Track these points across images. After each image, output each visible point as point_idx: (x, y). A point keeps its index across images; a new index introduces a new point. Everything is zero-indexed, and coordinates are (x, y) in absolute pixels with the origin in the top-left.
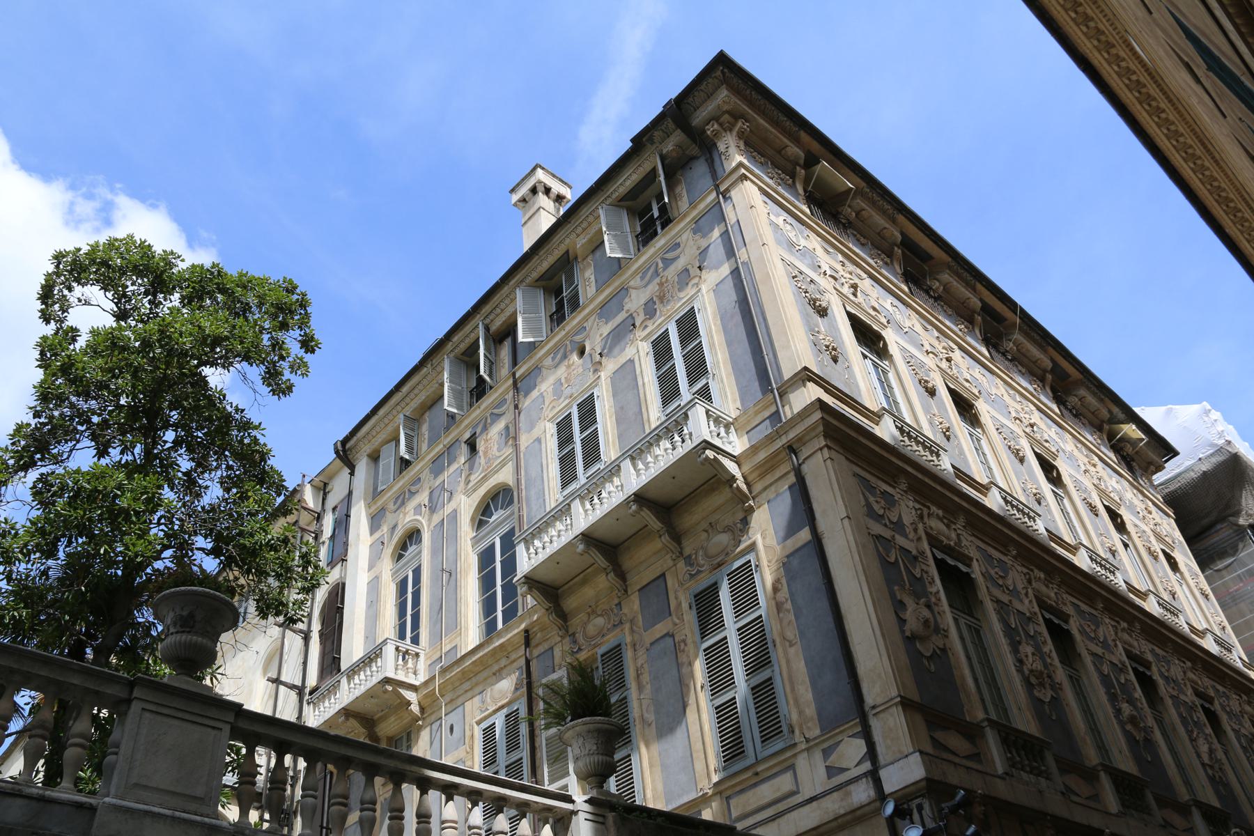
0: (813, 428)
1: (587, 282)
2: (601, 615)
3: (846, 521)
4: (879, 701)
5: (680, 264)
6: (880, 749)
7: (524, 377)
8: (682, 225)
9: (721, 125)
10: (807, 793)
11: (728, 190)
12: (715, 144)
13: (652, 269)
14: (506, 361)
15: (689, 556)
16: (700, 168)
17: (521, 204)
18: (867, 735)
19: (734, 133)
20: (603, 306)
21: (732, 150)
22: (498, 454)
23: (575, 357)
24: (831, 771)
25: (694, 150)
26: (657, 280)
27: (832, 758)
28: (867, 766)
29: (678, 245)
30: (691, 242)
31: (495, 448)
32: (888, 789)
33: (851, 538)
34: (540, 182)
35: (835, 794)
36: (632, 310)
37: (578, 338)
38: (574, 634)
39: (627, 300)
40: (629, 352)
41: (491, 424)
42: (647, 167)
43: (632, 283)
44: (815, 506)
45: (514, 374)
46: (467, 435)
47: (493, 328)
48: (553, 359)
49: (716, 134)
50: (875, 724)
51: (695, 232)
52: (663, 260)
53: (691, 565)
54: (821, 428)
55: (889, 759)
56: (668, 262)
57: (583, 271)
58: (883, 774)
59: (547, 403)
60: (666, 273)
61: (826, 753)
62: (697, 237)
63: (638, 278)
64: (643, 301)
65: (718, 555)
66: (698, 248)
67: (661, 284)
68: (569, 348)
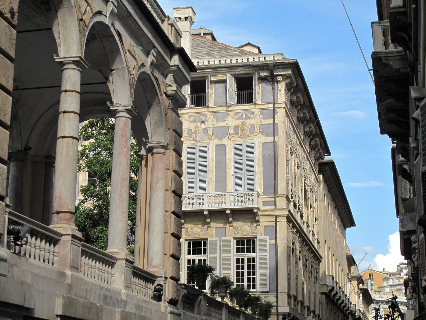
5: (253, 122)
13: (240, 115)
18: (277, 297)
25: (270, 79)
26: (242, 121)
32: (279, 311)
37: (203, 118)
40: (225, 141)
49: (280, 82)
55: (281, 305)
56: (247, 118)
58: (279, 308)
60: (246, 121)
62: (261, 116)
63: (234, 112)
67: (243, 124)
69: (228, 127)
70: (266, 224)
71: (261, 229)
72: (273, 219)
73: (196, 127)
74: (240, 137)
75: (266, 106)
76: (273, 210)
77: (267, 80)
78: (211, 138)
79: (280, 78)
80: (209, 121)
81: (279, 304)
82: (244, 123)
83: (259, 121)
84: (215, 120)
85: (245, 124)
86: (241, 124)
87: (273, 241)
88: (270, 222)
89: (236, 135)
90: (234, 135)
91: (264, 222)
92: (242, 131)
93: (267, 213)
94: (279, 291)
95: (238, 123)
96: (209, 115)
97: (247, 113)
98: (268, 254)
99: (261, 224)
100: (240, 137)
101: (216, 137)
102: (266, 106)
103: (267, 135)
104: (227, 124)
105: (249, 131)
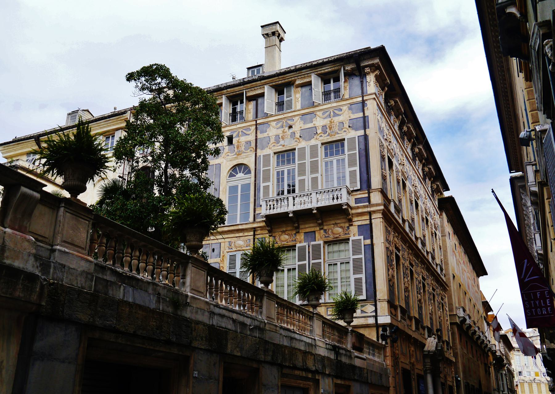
5: (341, 118)
7: (260, 124)
13: (328, 113)
14: (252, 111)
15: (326, 230)
16: (356, 81)
20: (303, 115)
21: (372, 84)
25: (357, 74)
30: (346, 112)
31: (243, 148)
37: (290, 123)
39: (314, 119)
43: (318, 113)
44: (374, 234)
47: (249, 94)
49: (368, 73)
51: (350, 109)
52: (334, 112)
56: (336, 115)
57: (295, 93)
66: (350, 117)
67: (331, 122)
70: (360, 223)
71: (354, 229)
72: (367, 217)
73: (283, 132)
75: (355, 100)
79: (367, 70)
83: (348, 116)
84: (302, 122)
86: (329, 122)
90: (322, 135)
91: (358, 221)
92: (330, 128)
93: (360, 211)
95: (326, 122)
97: (335, 111)
98: (362, 256)
101: (304, 139)
102: (355, 100)
103: (356, 129)
104: (314, 124)
105: (337, 128)
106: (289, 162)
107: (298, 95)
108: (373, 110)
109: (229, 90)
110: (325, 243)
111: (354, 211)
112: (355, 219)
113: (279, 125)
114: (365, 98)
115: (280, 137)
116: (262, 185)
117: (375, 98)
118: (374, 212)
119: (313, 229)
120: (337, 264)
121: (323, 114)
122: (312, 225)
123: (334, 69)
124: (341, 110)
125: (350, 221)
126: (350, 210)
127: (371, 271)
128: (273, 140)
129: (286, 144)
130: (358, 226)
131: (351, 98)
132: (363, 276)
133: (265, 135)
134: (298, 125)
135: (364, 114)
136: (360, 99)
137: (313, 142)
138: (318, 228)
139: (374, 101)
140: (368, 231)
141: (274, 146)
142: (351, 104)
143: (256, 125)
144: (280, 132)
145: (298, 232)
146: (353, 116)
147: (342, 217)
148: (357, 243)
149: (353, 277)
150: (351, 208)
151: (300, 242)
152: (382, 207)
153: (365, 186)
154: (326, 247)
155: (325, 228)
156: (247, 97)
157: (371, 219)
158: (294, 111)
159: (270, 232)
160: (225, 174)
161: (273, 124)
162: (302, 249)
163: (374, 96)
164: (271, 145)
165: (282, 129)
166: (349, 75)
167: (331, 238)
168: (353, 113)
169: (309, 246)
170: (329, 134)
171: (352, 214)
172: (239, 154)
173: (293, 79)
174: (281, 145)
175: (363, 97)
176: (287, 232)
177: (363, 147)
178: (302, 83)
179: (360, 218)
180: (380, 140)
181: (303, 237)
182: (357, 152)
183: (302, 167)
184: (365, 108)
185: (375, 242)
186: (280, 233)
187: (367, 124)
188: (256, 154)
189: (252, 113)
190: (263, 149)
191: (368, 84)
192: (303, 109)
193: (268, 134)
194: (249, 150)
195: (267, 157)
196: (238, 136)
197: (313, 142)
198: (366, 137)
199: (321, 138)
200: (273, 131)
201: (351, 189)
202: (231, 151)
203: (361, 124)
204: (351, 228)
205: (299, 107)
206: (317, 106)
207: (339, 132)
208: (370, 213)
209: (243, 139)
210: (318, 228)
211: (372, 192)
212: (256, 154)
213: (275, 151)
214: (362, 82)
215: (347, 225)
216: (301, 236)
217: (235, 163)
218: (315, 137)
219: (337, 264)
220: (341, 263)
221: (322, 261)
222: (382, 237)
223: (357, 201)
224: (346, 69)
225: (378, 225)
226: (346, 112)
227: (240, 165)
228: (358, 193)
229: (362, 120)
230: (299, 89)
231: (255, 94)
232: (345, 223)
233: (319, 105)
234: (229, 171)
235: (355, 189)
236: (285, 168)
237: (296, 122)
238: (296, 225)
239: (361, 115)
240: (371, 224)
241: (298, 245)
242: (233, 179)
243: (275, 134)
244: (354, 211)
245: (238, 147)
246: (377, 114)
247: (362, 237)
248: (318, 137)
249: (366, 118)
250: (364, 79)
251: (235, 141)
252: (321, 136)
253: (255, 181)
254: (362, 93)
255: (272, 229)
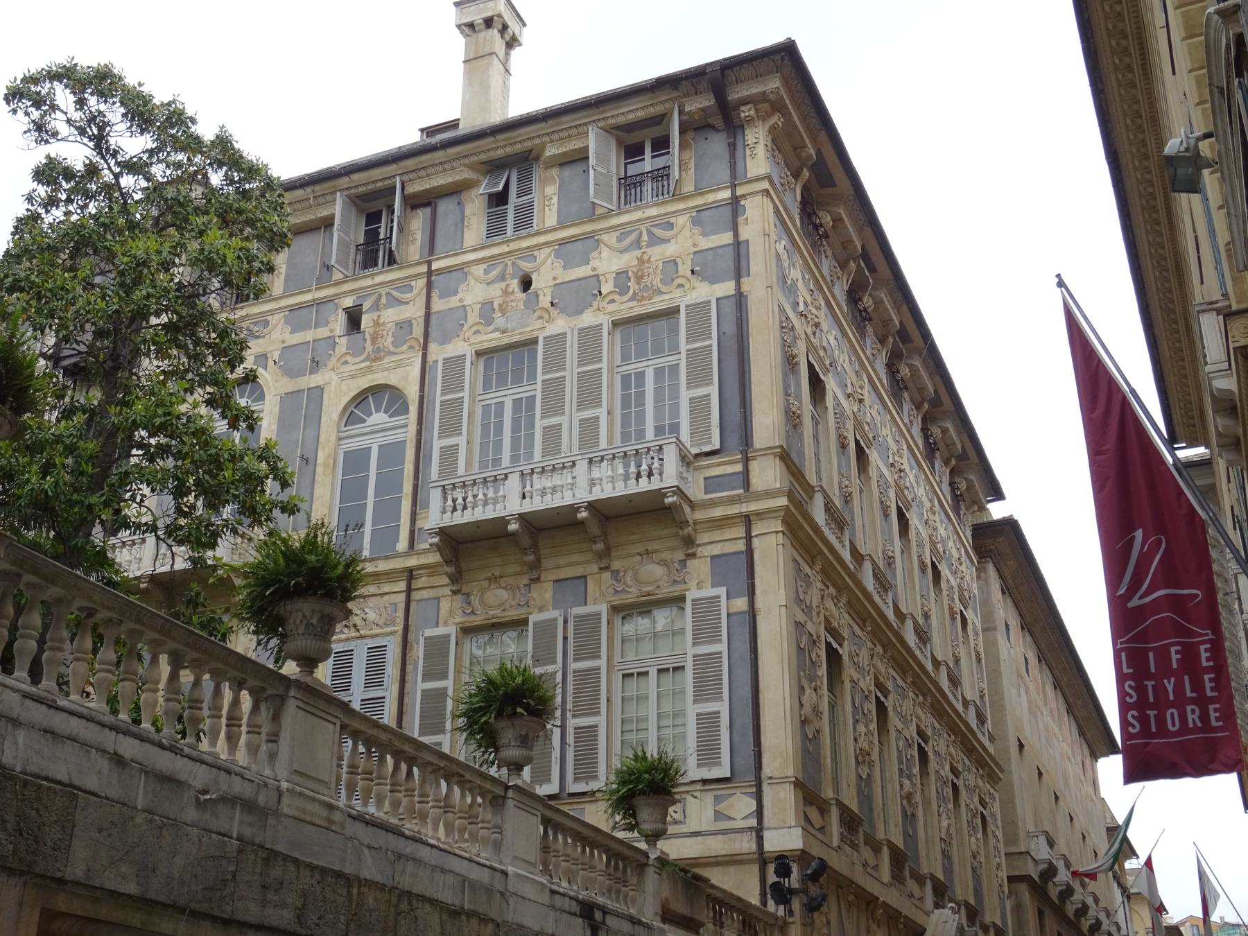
0: (774, 510)
1: (548, 198)
2: (505, 588)
3: (783, 609)
4: (776, 774)
5: (670, 250)
6: (767, 813)
7: (441, 271)
8: (682, 206)
9: (757, 111)
10: (692, 826)
11: (744, 196)
12: (742, 127)
14: (418, 236)
15: (618, 572)
16: (717, 144)
17: (467, 30)
19: (767, 127)
20: (563, 242)
21: (761, 150)
22: (392, 348)
23: (515, 284)
24: (719, 815)
25: (718, 121)
26: (638, 253)
27: (722, 805)
28: (753, 822)
29: (671, 226)
30: (686, 232)
31: (390, 339)
32: (768, 847)
33: (784, 627)
34: (499, 16)
35: (720, 837)
36: (600, 272)
37: (525, 266)
38: (468, 595)
39: (595, 254)
41: (387, 306)
42: (659, 109)
43: (605, 237)
44: (757, 582)
45: (429, 263)
46: (349, 302)
47: (410, 190)
48: (486, 272)
49: (750, 121)
50: (766, 789)
51: (696, 222)
52: (650, 233)
53: (618, 581)
54: (782, 513)
56: (655, 241)
57: (545, 182)
58: (767, 835)
59: (471, 320)
60: (651, 251)
61: (718, 800)
64: (615, 268)
65: (648, 583)
66: (695, 245)
67: (641, 261)
68: (510, 270)
69: (597, 276)
70: (717, 550)
71: (700, 568)
72: (740, 532)
73: (506, 292)
74: (633, 298)
75: (711, 198)
76: (737, 500)
77: (710, 127)
78: (546, 316)
79: (746, 112)
80: (542, 269)
81: (766, 820)
82: (646, 258)
83: (690, 242)
84: (559, 264)
85: (649, 261)
86: (635, 262)
87: (741, 604)
88: (729, 542)
89: (621, 294)
90: (616, 297)
92: (639, 279)
93: (718, 512)
94: (767, 770)
95: (628, 260)
96: (541, 255)
97: (655, 231)
98: (722, 647)
99: (702, 551)
100: (633, 298)
102: (711, 198)
103: (713, 280)
104: (594, 269)
105: (658, 278)
106: (517, 380)
107: (552, 190)
108: (760, 220)
109: (355, 177)
110: (615, 609)
111: (700, 515)
112: (703, 538)
113: (494, 273)
114: (739, 192)
115: (496, 306)
116: (437, 444)
117: (767, 191)
118: (760, 515)
119: (578, 571)
120: (646, 673)
121: (619, 240)
122: (577, 558)
123: (651, 110)
124: (671, 226)
125: (689, 542)
126: (687, 509)
127: (747, 693)
128: (473, 316)
129: (509, 326)
130: (712, 557)
131: (699, 192)
132: (723, 707)
133: (454, 301)
134: (549, 274)
135: (736, 235)
136: (726, 194)
137: (588, 319)
138: (594, 568)
139: (766, 200)
140: (742, 571)
141: (478, 332)
142: (700, 210)
143: (430, 273)
144: (495, 291)
145: (537, 580)
146: (705, 243)
147: (666, 532)
148: (706, 608)
149: (692, 711)
150: (693, 505)
151: (541, 609)
152: (783, 501)
153: (734, 440)
154: (618, 621)
155: (616, 565)
156: (406, 199)
157: (749, 538)
158: (538, 233)
159: (456, 579)
160: (335, 416)
161: (478, 270)
162: (546, 629)
163: (765, 185)
164: (467, 331)
165: (503, 285)
166: (694, 128)
167: (632, 596)
168: (704, 234)
169: (565, 622)
170: (634, 293)
171: (695, 523)
172: (376, 356)
173: (537, 141)
174: (497, 330)
175: (733, 187)
176: (503, 582)
177: (730, 328)
178: (564, 154)
179: (717, 535)
180: (782, 310)
181: (549, 595)
182: (714, 342)
183: (554, 390)
184: (741, 220)
185: (760, 602)
186: (485, 583)
187: (743, 263)
188: (424, 357)
189: (418, 243)
190: (445, 341)
191: (748, 152)
192: (562, 226)
193: (461, 300)
194: (405, 347)
195: (454, 364)
196: (376, 306)
197: (588, 319)
198: (740, 299)
199: (611, 308)
200: (473, 293)
201: (694, 451)
202: (355, 350)
203: (729, 264)
204: (691, 563)
205: (551, 219)
206: (605, 217)
207: (664, 289)
208: (747, 520)
209: (391, 315)
210: (594, 568)
211: (754, 458)
212: (424, 357)
213: (478, 347)
214: (732, 147)
215: (680, 555)
216: (545, 592)
217: (364, 383)
218: (595, 304)
219: (646, 673)
220: (660, 671)
221: (602, 663)
222: (782, 591)
223: (711, 484)
224: (687, 109)
225: (772, 553)
226: (686, 232)
227: (376, 391)
228: (714, 460)
229: (730, 253)
230: (555, 172)
231: (427, 186)
232: (673, 549)
233: (609, 214)
234: (345, 409)
235: (706, 449)
236: (507, 397)
237: (543, 263)
238: (531, 557)
239: (727, 238)
240: (750, 552)
241: (533, 619)
242: (356, 429)
243: (480, 299)
244: (700, 515)
245: (374, 339)
246: (774, 237)
247: (722, 591)
248: (603, 304)
249: (743, 248)
250: (739, 138)
251: (366, 321)
252: (613, 301)
253: (419, 432)
254: (734, 175)
255: (460, 571)
